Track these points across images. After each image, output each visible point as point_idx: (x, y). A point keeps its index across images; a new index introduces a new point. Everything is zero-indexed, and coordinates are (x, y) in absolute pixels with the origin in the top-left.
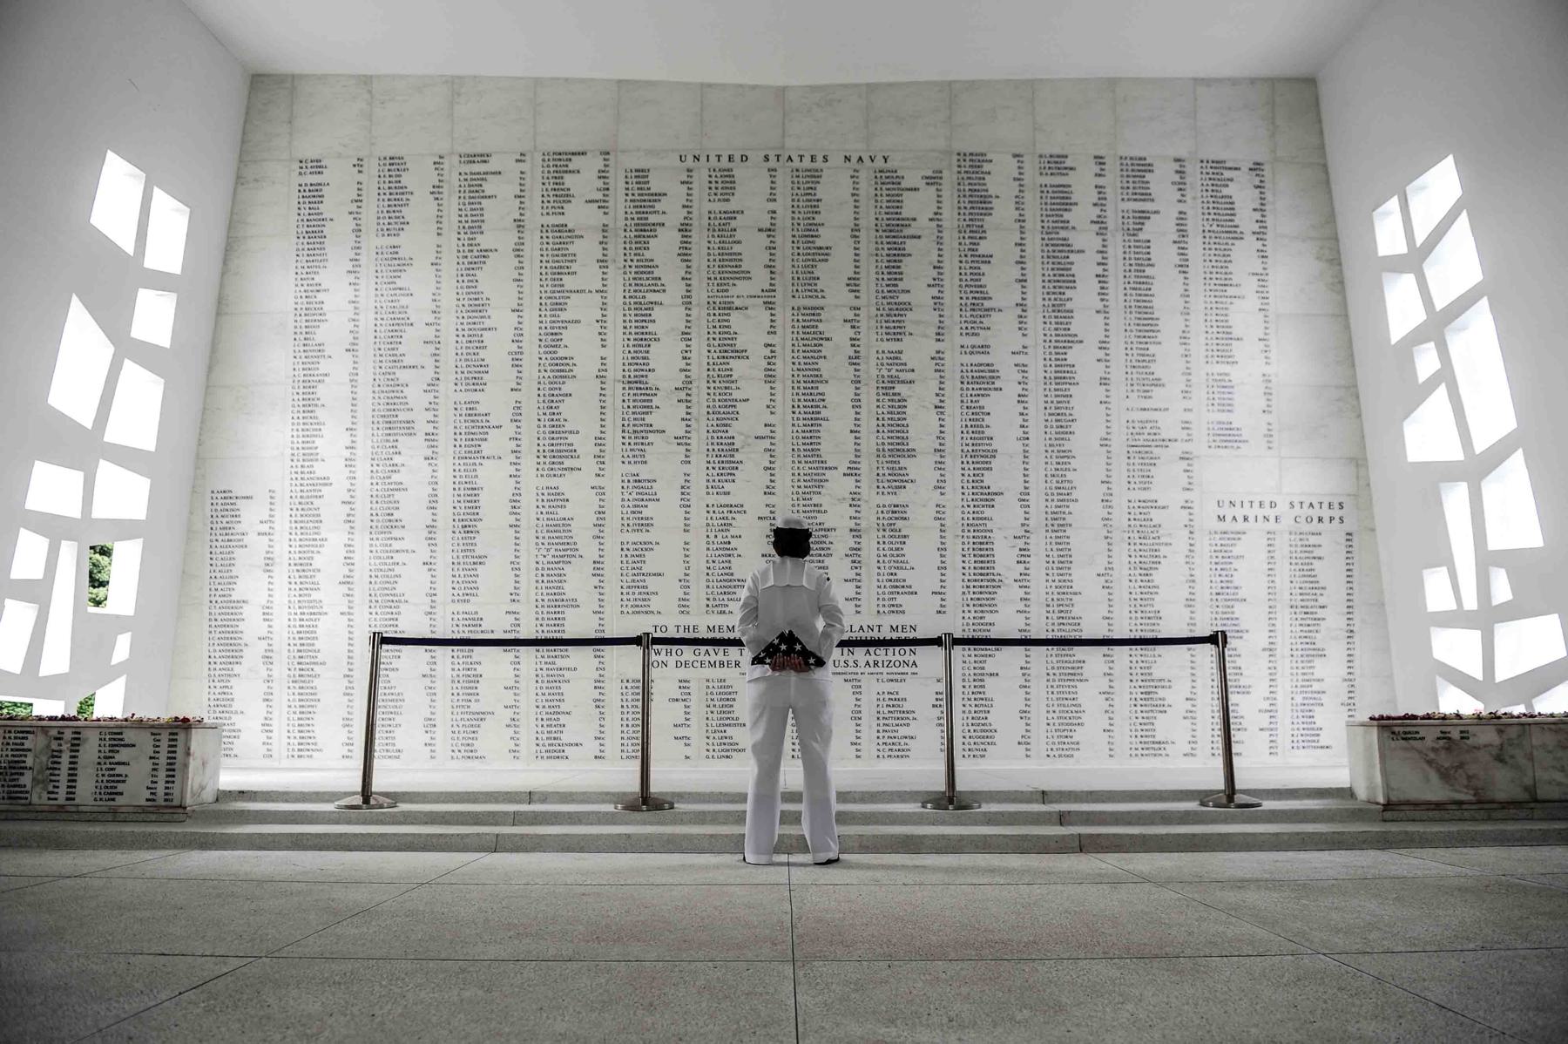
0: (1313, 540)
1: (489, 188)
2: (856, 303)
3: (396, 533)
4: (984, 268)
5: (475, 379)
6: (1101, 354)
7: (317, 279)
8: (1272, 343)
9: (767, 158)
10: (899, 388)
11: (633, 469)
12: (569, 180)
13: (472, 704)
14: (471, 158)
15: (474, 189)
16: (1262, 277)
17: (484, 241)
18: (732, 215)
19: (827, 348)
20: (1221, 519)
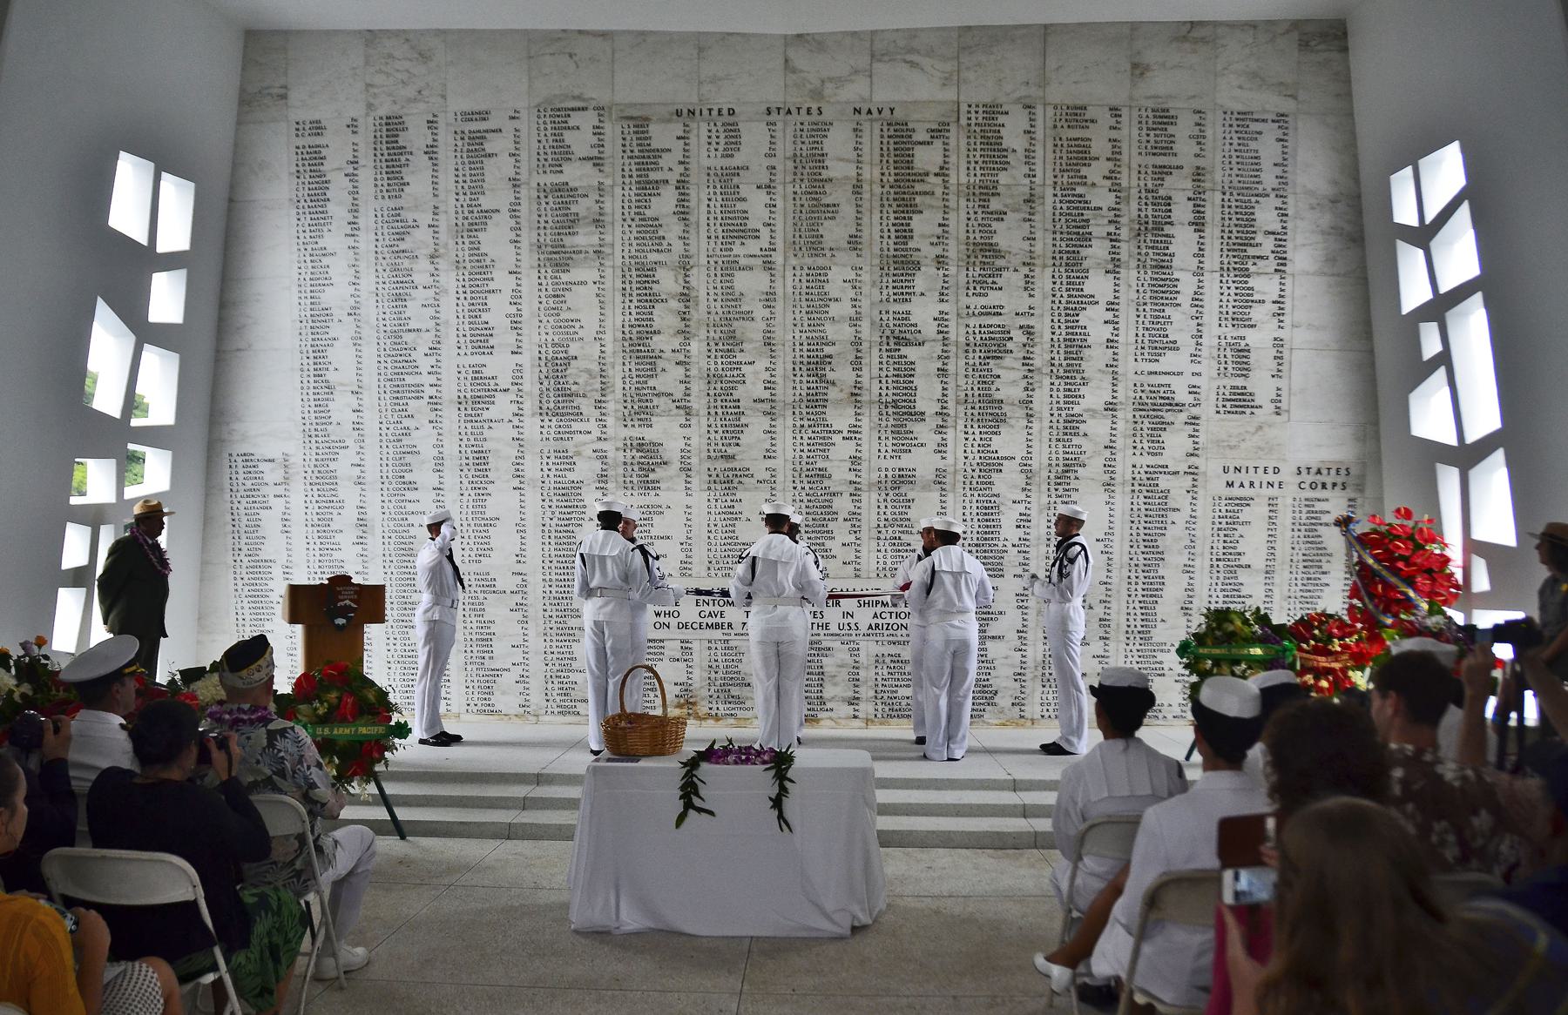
0: (1319, 506)
1: (489, 148)
2: (859, 262)
3: (410, 495)
4: (995, 225)
5: (482, 341)
6: (1109, 316)
8: (1288, 306)
9: (769, 112)
10: (904, 351)
11: (637, 432)
12: (569, 137)
13: (486, 661)
14: (469, 116)
15: (475, 147)
16: (1280, 237)
17: (486, 202)
18: (736, 171)
19: (834, 310)
20: (1230, 485)
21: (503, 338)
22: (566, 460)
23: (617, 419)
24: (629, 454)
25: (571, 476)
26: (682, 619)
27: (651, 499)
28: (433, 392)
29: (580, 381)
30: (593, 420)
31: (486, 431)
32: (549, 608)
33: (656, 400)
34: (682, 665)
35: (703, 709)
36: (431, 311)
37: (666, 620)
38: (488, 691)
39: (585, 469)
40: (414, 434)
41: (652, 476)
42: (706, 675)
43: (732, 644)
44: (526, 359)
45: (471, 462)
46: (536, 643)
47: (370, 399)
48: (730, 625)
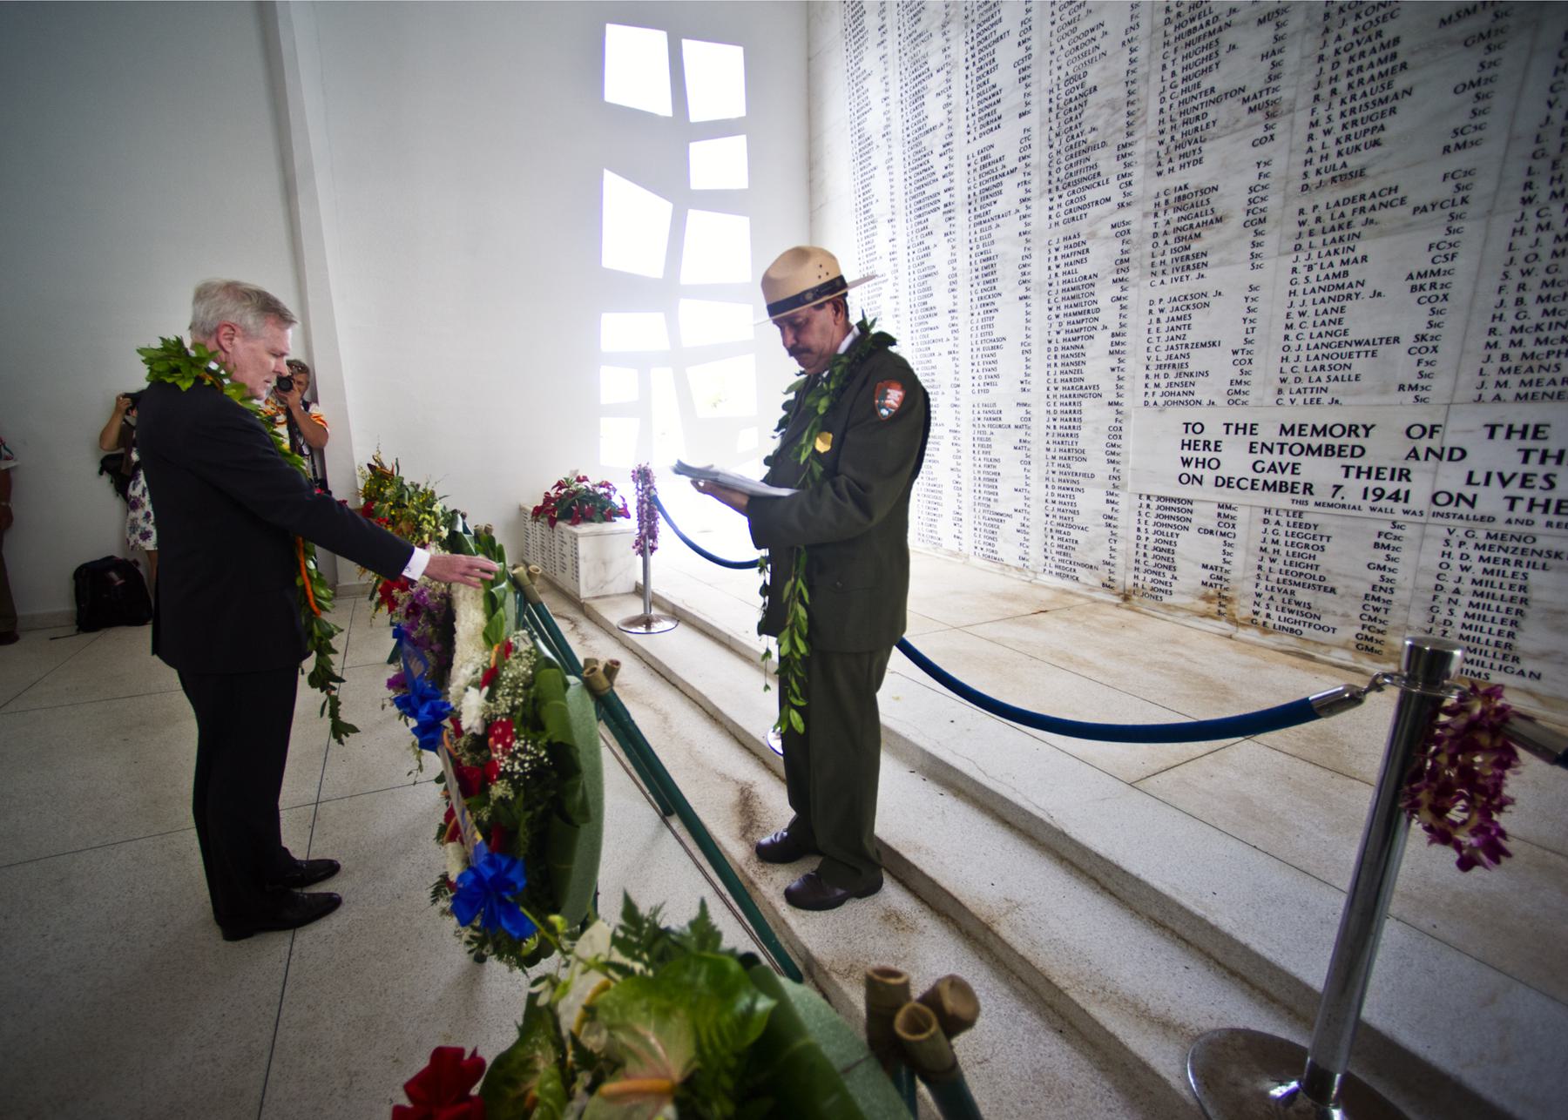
3: (932, 322)
7: (863, 65)
13: (992, 503)
21: (1012, 99)
22: (1077, 248)
23: (1148, 165)
24: (1161, 219)
25: (1083, 270)
26: (1224, 472)
27: (1191, 284)
28: (945, 198)
29: (1099, 123)
30: (1113, 179)
31: (993, 232)
32: (1052, 446)
33: (1213, 112)
34: (1217, 541)
35: (1243, 609)
36: (943, 99)
37: (1199, 472)
38: (992, 536)
39: (1101, 257)
40: (933, 252)
41: (1196, 247)
42: (1256, 562)
43: (1306, 519)
44: (1033, 120)
45: (980, 273)
46: (1038, 490)
47: (901, 224)
48: (1308, 488)
